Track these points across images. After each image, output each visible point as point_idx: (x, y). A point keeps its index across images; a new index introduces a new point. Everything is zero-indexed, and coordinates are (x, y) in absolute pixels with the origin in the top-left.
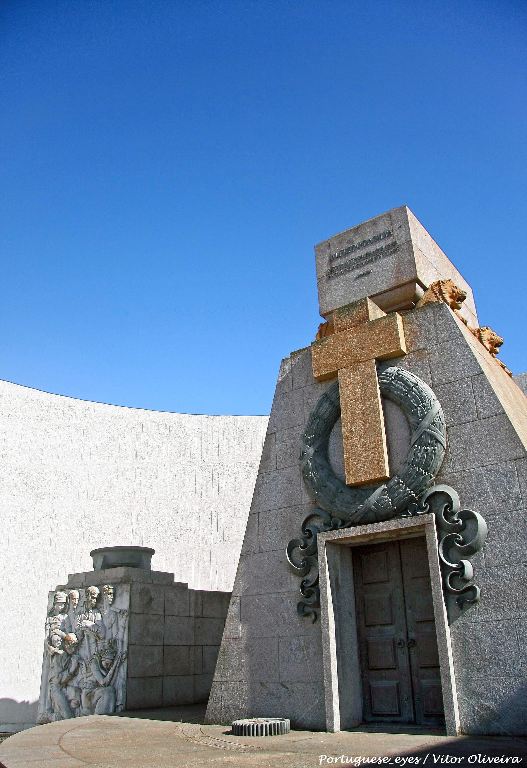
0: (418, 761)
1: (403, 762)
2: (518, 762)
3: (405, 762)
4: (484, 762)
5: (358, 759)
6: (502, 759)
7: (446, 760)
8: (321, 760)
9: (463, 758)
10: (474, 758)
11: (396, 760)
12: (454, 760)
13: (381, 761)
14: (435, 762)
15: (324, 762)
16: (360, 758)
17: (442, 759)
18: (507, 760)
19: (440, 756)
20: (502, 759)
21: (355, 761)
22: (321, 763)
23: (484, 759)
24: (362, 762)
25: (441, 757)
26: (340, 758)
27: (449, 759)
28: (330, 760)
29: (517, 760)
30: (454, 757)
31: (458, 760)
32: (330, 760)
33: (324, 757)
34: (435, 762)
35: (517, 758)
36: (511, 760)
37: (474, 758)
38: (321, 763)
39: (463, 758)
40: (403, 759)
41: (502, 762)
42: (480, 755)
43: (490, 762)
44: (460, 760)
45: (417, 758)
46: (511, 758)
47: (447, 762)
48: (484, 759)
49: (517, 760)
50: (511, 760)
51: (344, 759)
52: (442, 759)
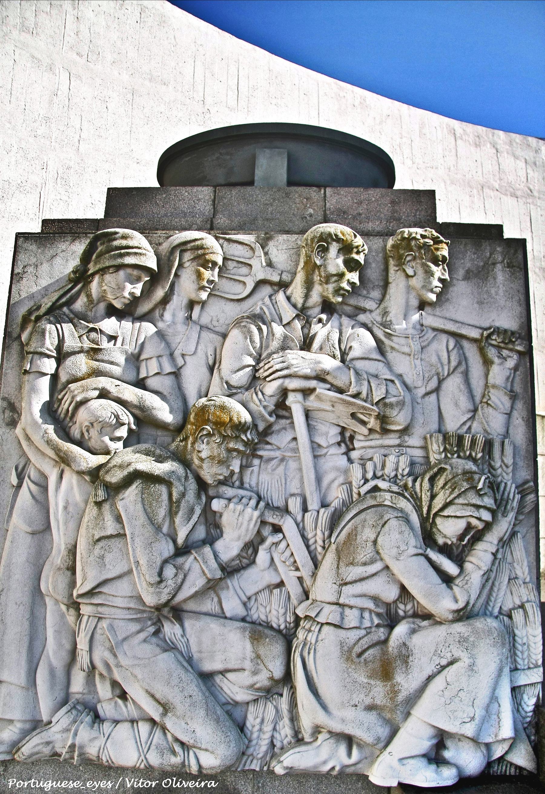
0: (110, 785)
1: (94, 787)
2: (214, 786)
3: (97, 786)
4: (179, 786)
5: (48, 783)
6: (197, 783)
7: (140, 784)
8: (10, 784)
9: (158, 782)
10: (168, 782)
11: (88, 784)
12: (147, 784)
13: (72, 785)
14: (129, 786)
15: (14, 786)
16: (50, 782)
17: (135, 783)
18: (203, 784)
19: (133, 780)
20: (197, 783)
21: (45, 785)
22: (10, 787)
23: (179, 783)
24: (52, 787)
25: (134, 781)
26: (30, 782)
27: (143, 783)
28: (20, 784)
29: (213, 784)
30: (148, 781)
32: (20, 784)
33: (13, 782)
34: (129, 786)
35: (213, 782)
36: (206, 784)
37: (168, 782)
38: (10, 787)
39: (158, 782)
40: (95, 783)
41: (197, 786)
42: (175, 779)
43: (185, 786)
44: (154, 784)
45: (110, 782)
46: (207, 782)
48: (179, 783)
49: (213, 784)
50: (206, 784)
51: (35, 783)
52: (135, 783)
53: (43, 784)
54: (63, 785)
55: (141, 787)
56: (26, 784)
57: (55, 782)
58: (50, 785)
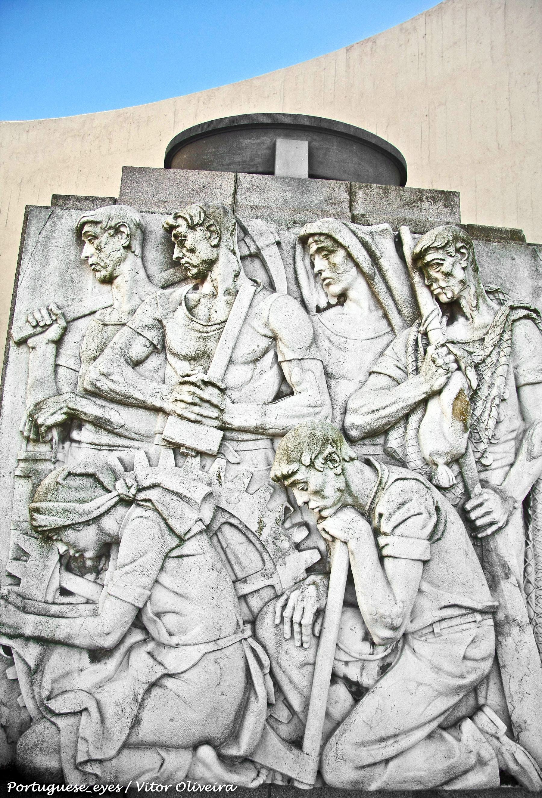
0: (119, 789)
1: (102, 790)
2: (232, 790)
3: (104, 790)
4: (194, 791)
5: (51, 787)
7: (151, 788)
8: (10, 788)
10: (182, 785)
11: (94, 788)
12: (160, 788)
13: (77, 789)
14: (139, 790)
15: (14, 790)
16: (53, 785)
17: (146, 787)
21: (48, 789)
22: (9, 791)
24: (55, 791)
26: (31, 785)
28: (20, 788)
29: (231, 788)
31: (24, 788)
32: (20, 788)
33: (13, 785)
34: (139, 790)
37: (182, 785)
38: (9, 791)
40: (102, 787)
41: (214, 791)
42: (189, 782)
43: (201, 790)
45: (118, 785)
47: (63, 790)
49: (231, 788)
51: (36, 787)
53: (46, 788)
54: (67, 789)
55: (152, 791)
56: (27, 788)
57: (58, 786)
58: (53, 789)
